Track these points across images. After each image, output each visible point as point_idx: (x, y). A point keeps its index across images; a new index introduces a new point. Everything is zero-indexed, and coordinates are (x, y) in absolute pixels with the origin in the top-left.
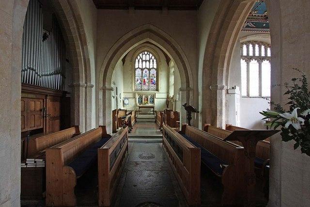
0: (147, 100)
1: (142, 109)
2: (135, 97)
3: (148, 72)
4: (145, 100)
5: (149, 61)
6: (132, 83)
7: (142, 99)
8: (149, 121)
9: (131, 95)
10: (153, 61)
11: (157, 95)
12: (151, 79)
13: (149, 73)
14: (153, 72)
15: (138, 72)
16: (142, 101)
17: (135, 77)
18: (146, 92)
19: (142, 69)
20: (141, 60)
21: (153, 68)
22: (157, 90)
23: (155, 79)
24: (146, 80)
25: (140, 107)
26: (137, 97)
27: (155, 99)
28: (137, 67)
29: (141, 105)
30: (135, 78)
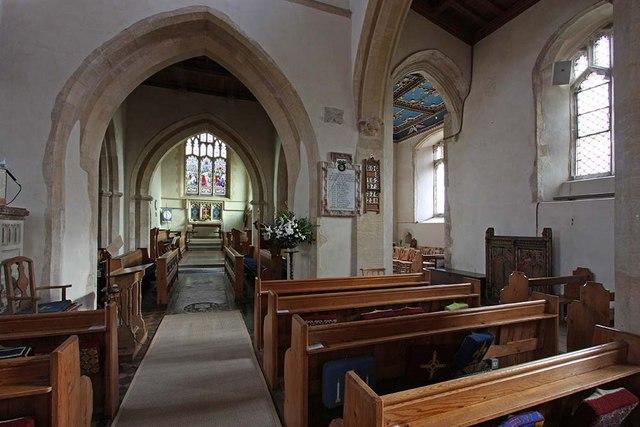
0: (209, 213)
1: (198, 230)
3: (210, 164)
4: (204, 213)
5: (213, 144)
6: (179, 181)
8: (211, 248)
9: (177, 204)
10: (220, 145)
11: (228, 205)
13: (213, 165)
14: (221, 164)
15: (191, 162)
16: (198, 215)
17: (185, 169)
18: (206, 198)
19: (200, 158)
20: (196, 141)
21: (220, 157)
22: (227, 196)
23: (224, 177)
24: (207, 178)
25: (194, 225)
26: (189, 207)
27: (224, 213)
28: (188, 152)
29: (197, 222)
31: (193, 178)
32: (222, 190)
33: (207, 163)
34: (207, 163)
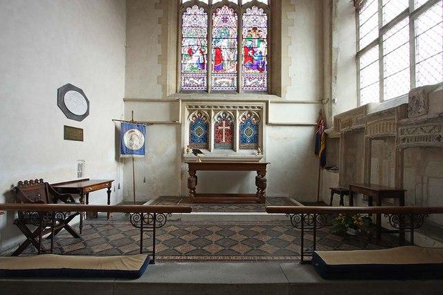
2: (174, 122)
7: (207, 127)
11: (276, 113)
12: (247, 49)
13: (240, 24)
17: (179, 38)
23: (262, 48)
24: (225, 54)
26: (186, 119)
27: (268, 132)
30: (178, 45)
31: (197, 57)
32: (260, 80)
33: (225, 20)
34: (225, 20)
